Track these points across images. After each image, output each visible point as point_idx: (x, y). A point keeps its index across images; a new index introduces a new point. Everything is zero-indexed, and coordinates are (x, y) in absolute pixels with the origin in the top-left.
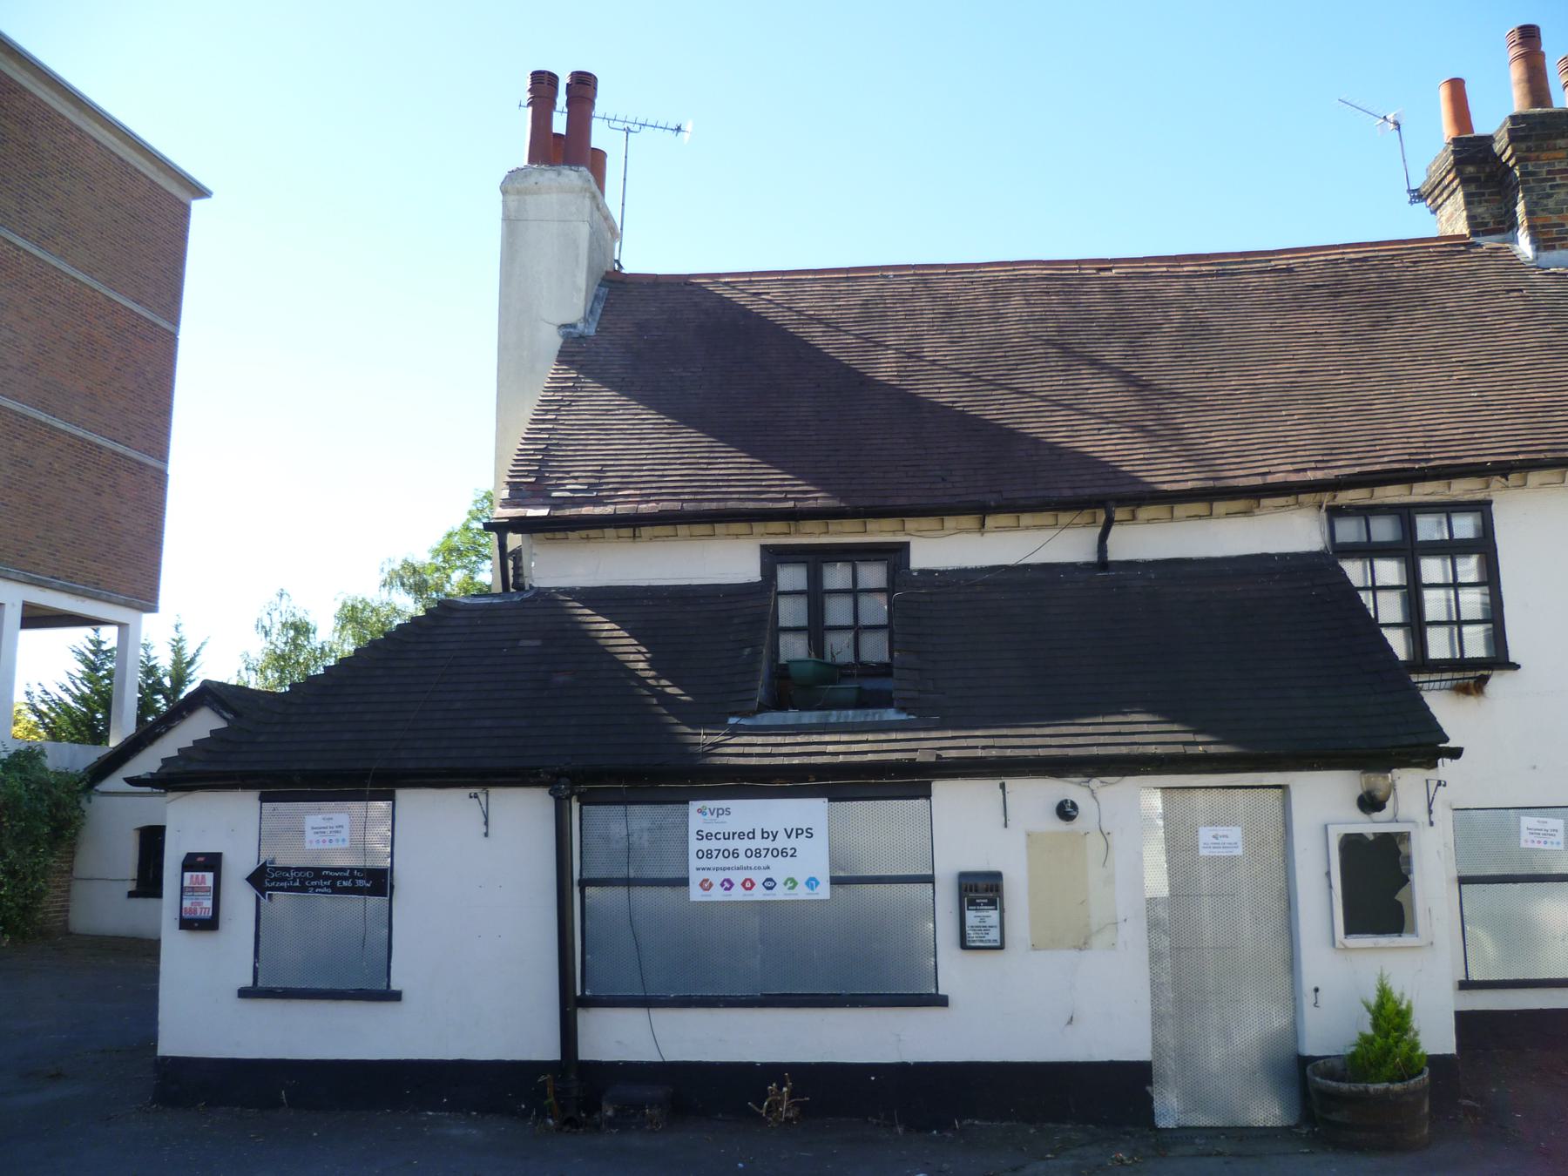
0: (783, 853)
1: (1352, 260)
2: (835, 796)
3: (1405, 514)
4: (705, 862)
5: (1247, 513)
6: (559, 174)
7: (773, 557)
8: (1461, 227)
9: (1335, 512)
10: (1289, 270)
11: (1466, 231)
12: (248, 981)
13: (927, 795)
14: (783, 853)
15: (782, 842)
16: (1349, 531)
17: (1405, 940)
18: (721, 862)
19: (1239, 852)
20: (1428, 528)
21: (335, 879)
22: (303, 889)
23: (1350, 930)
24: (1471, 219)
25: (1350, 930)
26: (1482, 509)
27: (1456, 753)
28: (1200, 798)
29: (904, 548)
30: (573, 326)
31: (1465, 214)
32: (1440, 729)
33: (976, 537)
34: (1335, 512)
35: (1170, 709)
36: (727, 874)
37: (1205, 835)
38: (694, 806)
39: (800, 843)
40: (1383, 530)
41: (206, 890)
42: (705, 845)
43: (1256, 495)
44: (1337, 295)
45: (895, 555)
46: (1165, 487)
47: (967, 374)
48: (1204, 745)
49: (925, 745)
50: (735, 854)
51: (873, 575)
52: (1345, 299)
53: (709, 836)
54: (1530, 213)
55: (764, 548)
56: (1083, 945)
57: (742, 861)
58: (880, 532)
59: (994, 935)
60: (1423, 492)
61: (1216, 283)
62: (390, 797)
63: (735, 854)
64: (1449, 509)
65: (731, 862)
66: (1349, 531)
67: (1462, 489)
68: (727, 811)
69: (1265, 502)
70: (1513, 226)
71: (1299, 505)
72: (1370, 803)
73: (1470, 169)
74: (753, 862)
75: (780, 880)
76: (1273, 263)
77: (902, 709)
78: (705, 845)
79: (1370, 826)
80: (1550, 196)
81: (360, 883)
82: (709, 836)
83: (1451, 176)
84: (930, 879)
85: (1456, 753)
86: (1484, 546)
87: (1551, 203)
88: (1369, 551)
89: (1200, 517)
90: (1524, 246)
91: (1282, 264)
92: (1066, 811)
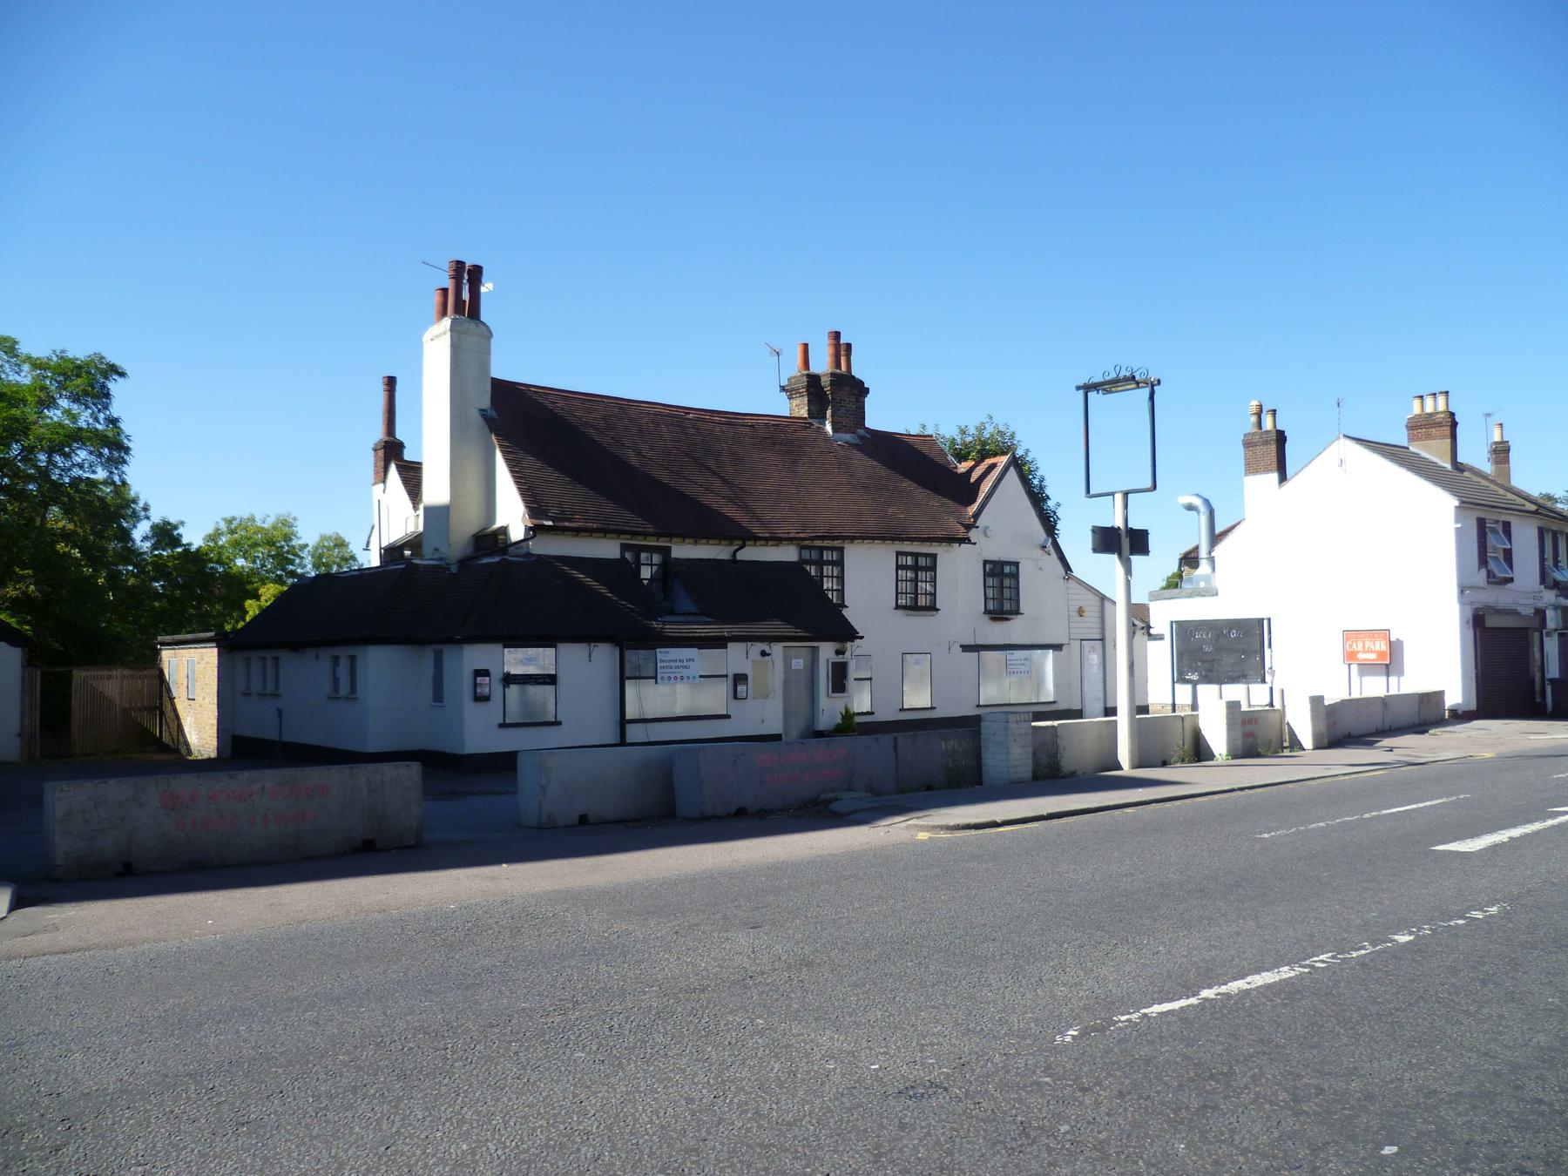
0: (685, 667)
1: (774, 425)
2: (700, 648)
3: (821, 549)
4: (662, 671)
5: (777, 545)
6: (477, 326)
7: (624, 548)
8: (804, 413)
9: (803, 548)
10: (752, 426)
11: (806, 416)
12: (502, 721)
13: (726, 648)
14: (685, 667)
15: (685, 663)
16: (806, 555)
17: (845, 694)
18: (667, 670)
19: (802, 667)
20: (827, 556)
21: (537, 679)
22: (524, 683)
23: (833, 692)
24: (809, 410)
25: (833, 692)
26: (841, 550)
27: (862, 638)
28: (793, 650)
29: (669, 549)
30: (485, 410)
31: (807, 408)
32: (855, 630)
33: (692, 547)
34: (803, 548)
35: (788, 621)
36: (674, 675)
37: (794, 661)
38: (658, 650)
39: (691, 663)
40: (814, 555)
41: (486, 684)
42: (663, 664)
43: (778, 540)
44: (774, 444)
45: (666, 551)
46: (760, 535)
47: (713, 492)
48: (788, 630)
49: (725, 630)
50: (671, 667)
51: (656, 559)
52: (778, 447)
53: (663, 661)
54: (832, 416)
55: (621, 544)
56: (767, 697)
57: (674, 670)
58: (663, 543)
59: (745, 694)
60: (826, 543)
61: (724, 428)
62: (556, 647)
63: (671, 667)
64: (832, 549)
65: (671, 670)
66: (806, 555)
67: (836, 543)
68: (668, 652)
69: (784, 542)
70: (824, 417)
71: (792, 544)
72: (839, 652)
73: (812, 390)
74: (677, 670)
75: (685, 677)
76: (746, 421)
77: (708, 617)
78: (663, 664)
79: (840, 659)
80: (839, 410)
81: (547, 680)
82: (663, 661)
83: (804, 390)
84: (726, 676)
85: (862, 638)
86: (840, 563)
87: (839, 413)
88: (811, 562)
89: (763, 545)
90: (828, 428)
91: (750, 422)
92: (764, 654)
